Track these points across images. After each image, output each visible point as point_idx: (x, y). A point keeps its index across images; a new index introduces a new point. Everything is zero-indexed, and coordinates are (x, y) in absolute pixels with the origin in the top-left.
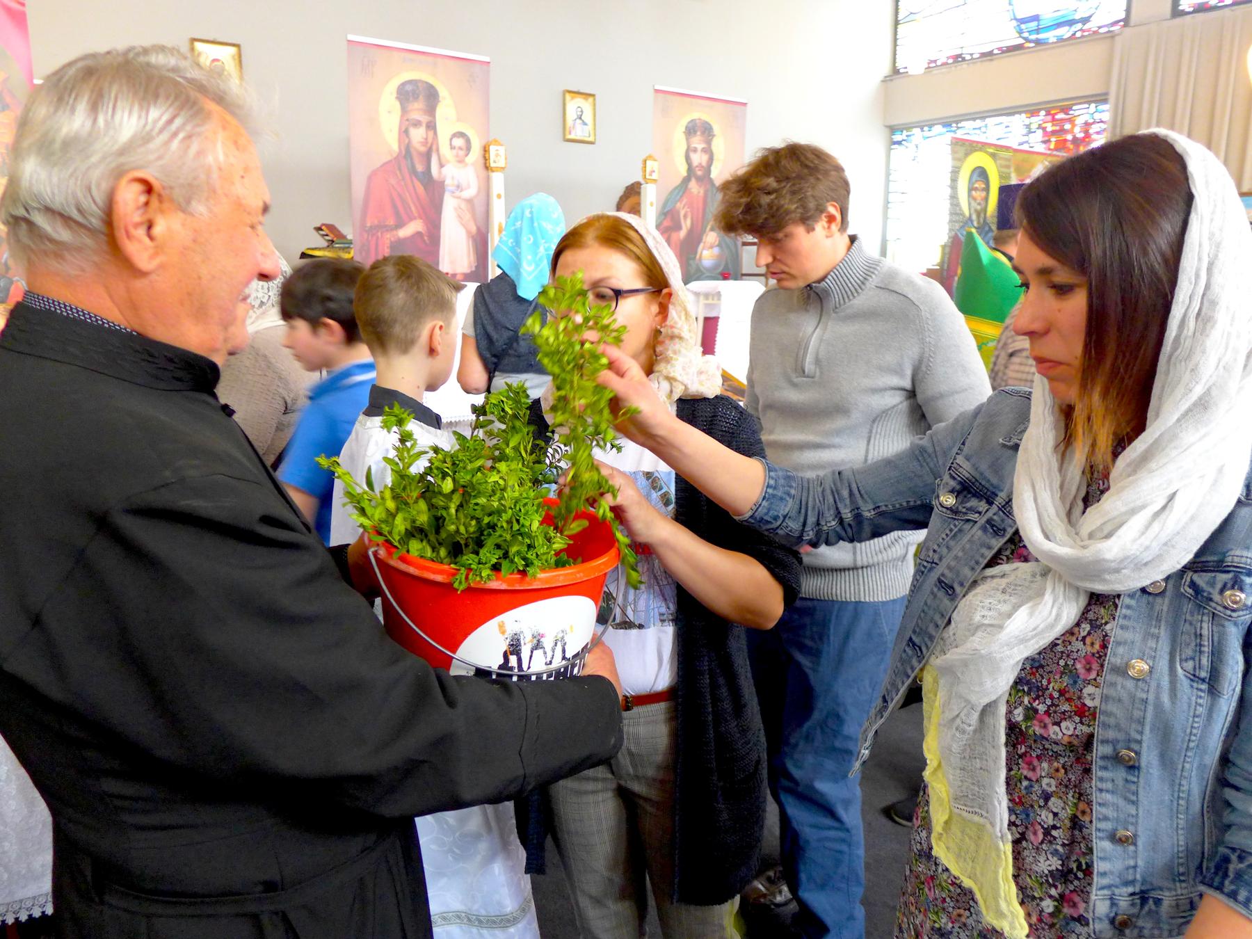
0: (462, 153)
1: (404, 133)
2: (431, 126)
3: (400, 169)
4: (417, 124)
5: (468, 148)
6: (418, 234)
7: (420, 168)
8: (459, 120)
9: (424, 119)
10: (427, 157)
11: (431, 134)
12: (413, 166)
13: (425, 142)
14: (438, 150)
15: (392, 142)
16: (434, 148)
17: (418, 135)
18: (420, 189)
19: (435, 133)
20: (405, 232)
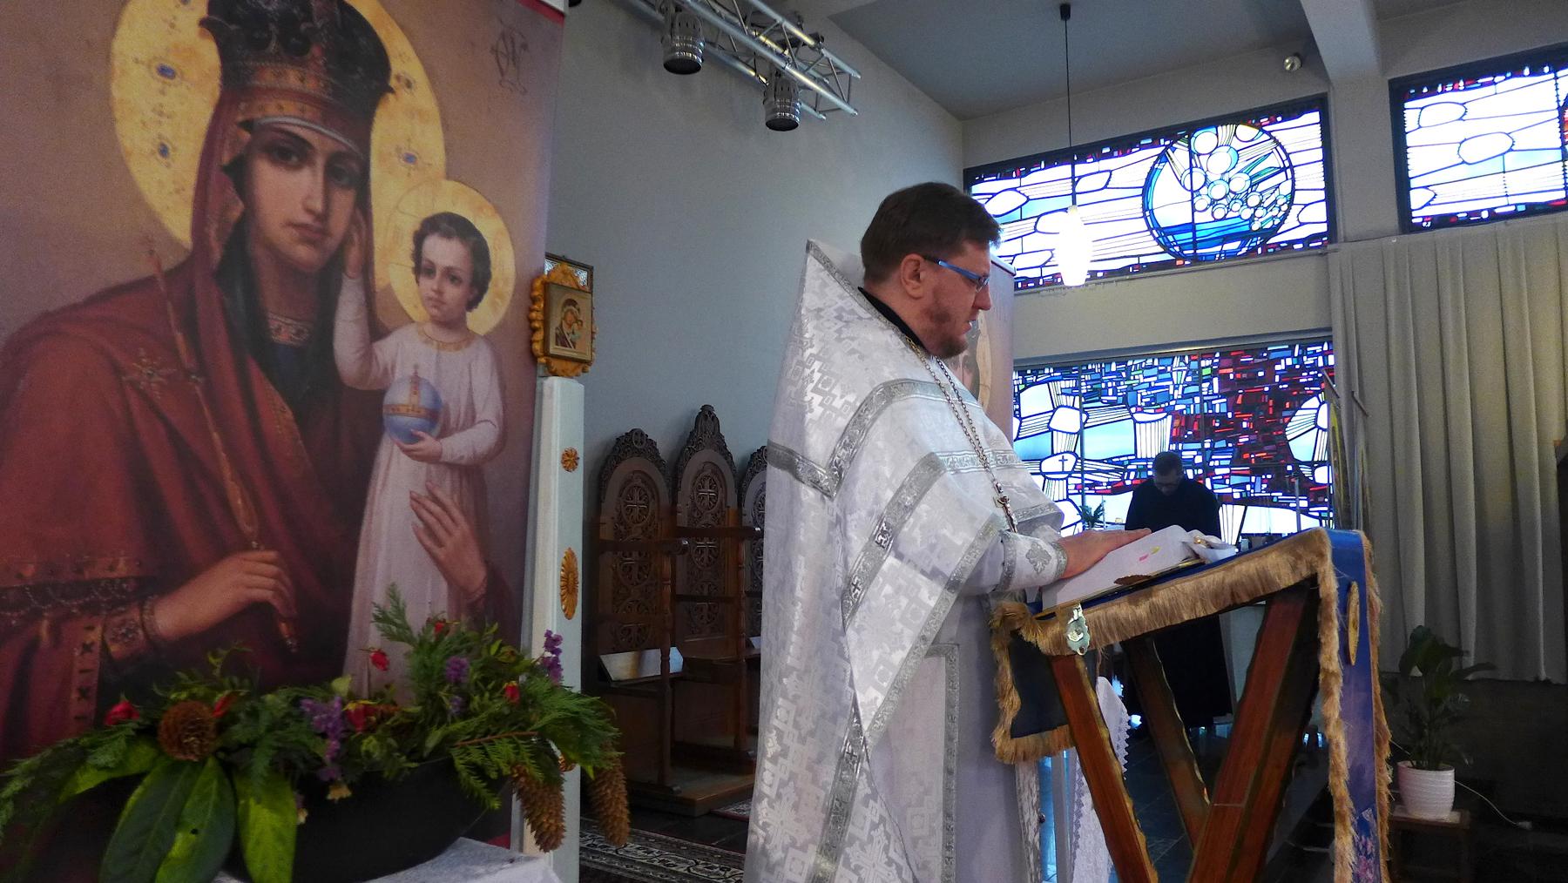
0: (453, 293)
1: (226, 170)
2: (350, 173)
3: (190, 326)
4: (290, 152)
5: (478, 282)
6: (252, 614)
7: (284, 330)
8: (450, 175)
9: (324, 140)
10: (319, 290)
11: (344, 201)
12: (257, 319)
13: (316, 231)
14: (366, 268)
15: (167, 193)
16: (354, 255)
17: (287, 194)
18: (278, 416)
19: (363, 205)
20: (173, 616)
